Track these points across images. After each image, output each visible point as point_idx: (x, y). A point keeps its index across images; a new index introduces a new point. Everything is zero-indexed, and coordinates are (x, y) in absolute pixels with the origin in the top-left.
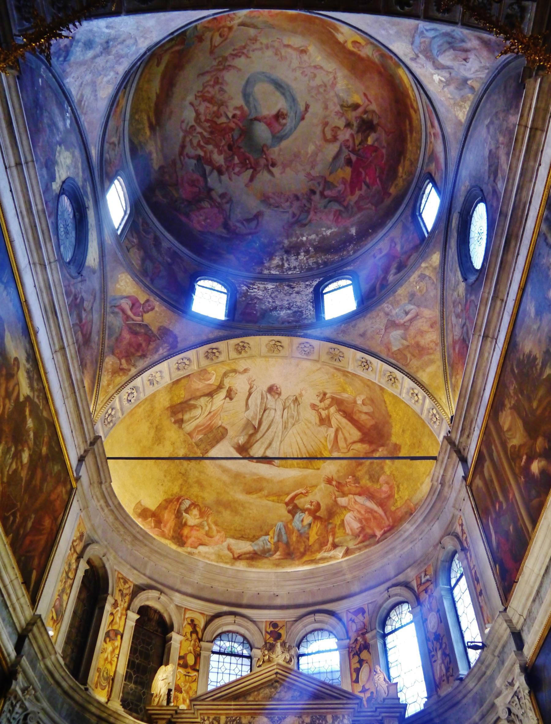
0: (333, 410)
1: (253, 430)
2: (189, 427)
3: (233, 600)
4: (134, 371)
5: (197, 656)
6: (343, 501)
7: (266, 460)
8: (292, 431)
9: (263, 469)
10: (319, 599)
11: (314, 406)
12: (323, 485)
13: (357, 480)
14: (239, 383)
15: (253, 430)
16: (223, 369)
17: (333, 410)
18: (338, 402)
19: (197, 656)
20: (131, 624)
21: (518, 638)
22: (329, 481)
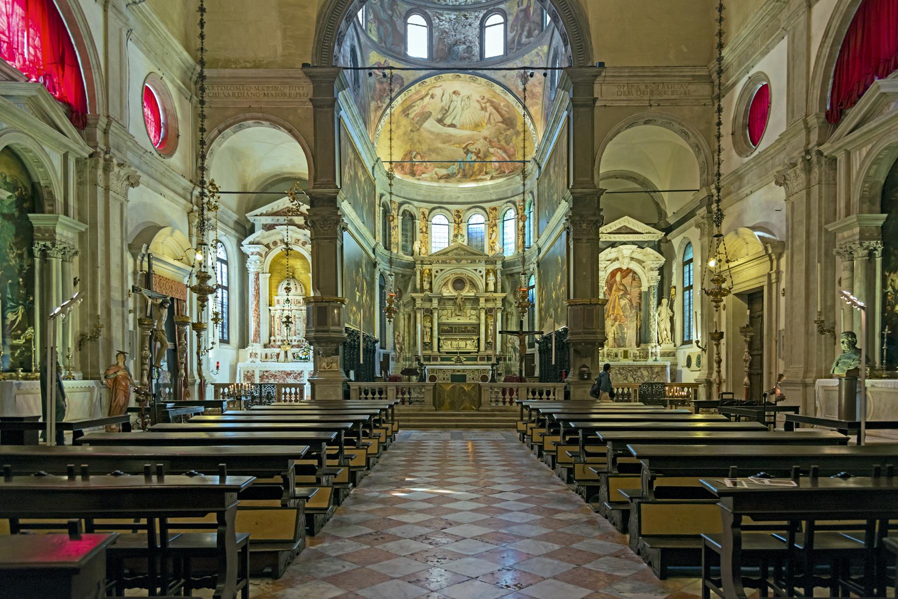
0: (488, 104)
1: (445, 111)
2: (411, 116)
3: (439, 200)
4: (385, 106)
5: (427, 228)
6: (491, 150)
7: (453, 126)
8: (466, 112)
9: (451, 130)
10: (478, 200)
11: (478, 101)
12: (482, 140)
13: (499, 141)
14: (438, 92)
15: (445, 111)
16: (428, 88)
17: (488, 104)
18: (492, 103)
19: (427, 228)
20: (400, 221)
21: (539, 250)
22: (485, 139)
